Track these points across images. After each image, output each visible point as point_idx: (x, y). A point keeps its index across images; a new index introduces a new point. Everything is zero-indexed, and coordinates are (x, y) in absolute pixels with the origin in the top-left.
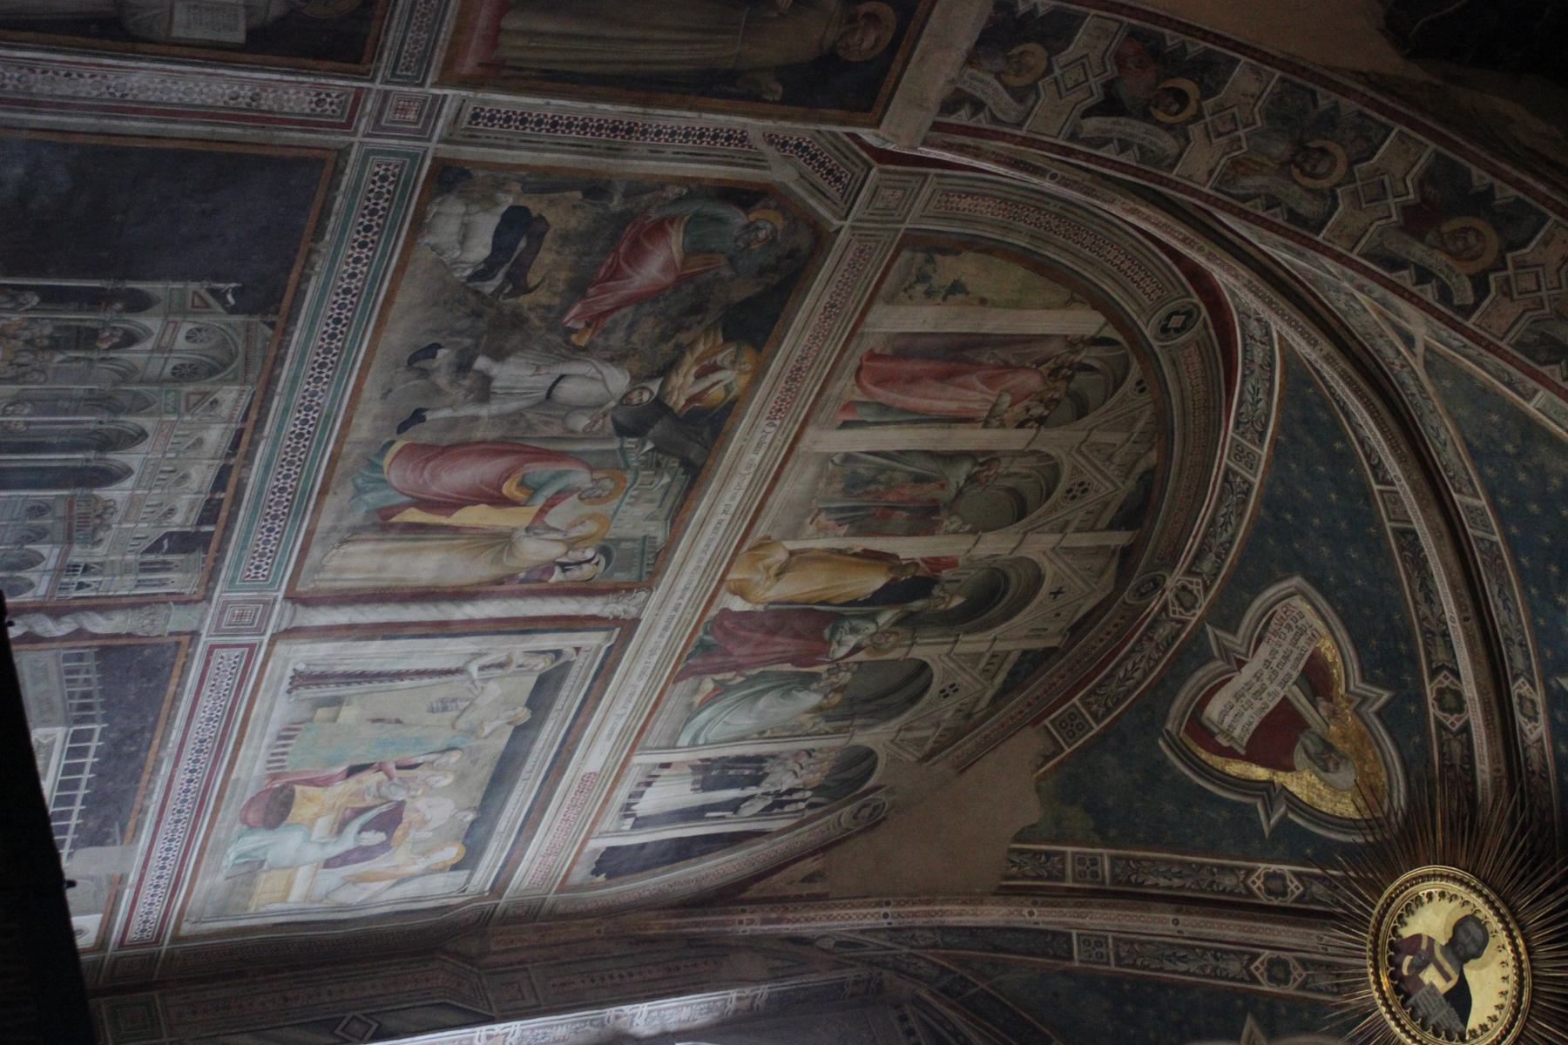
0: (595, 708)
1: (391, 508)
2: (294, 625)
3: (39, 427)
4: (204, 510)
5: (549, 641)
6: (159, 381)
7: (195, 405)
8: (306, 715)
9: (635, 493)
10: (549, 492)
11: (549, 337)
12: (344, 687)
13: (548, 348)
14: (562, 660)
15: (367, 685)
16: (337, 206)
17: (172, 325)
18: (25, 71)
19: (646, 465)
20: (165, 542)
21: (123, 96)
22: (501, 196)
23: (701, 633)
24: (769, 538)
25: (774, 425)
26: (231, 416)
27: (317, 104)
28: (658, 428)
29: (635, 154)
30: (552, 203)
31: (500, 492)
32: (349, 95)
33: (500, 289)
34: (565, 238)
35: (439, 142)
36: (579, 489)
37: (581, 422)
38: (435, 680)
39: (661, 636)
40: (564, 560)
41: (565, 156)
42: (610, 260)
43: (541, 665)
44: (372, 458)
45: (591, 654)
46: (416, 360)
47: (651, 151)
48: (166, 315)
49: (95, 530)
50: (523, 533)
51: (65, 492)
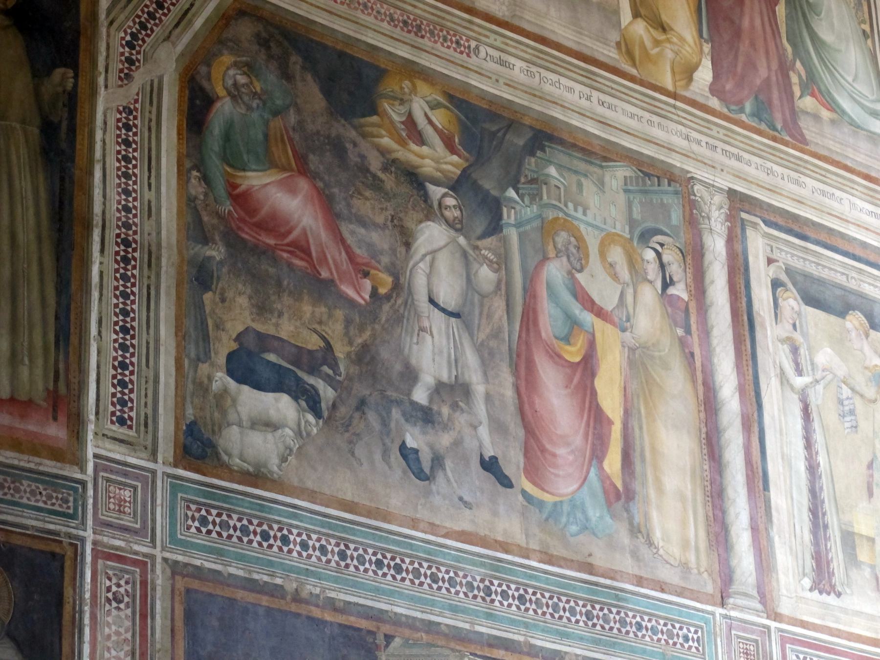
0: (843, 236)
1: (606, 492)
2: (756, 595)
5: (761, 294)
8: (867, 572)
9: (570, 205)
10: (577, 310)
11: (384, 319)
12: (830, 531)
13: (398, 319)
14: (784, 277)
15: (826, 505)
16: (241, 573)
19: (535, 197)
22: (215, 386)
23: (743, 117)
24: (618, 44)
25: (477, 47)
27: (120, 602)
28: (488, 184)
29: (154, 234)
30: (218, 327)
31: (579, 363)
32: (106, 567)
33: (330, 381)
34: (262, 309)
35: (155, 461)
36: (570, 273)
37: (486, 275)
38: (816, 425)
39: (749, 163)
40: (659, 284)
41: (162, 314)
42: (285, 255)
43: (792, 302)
44: (544, 516)
45: (774, 245)
46: (422, 471)
47: (150, 215)
50: (628, 334)
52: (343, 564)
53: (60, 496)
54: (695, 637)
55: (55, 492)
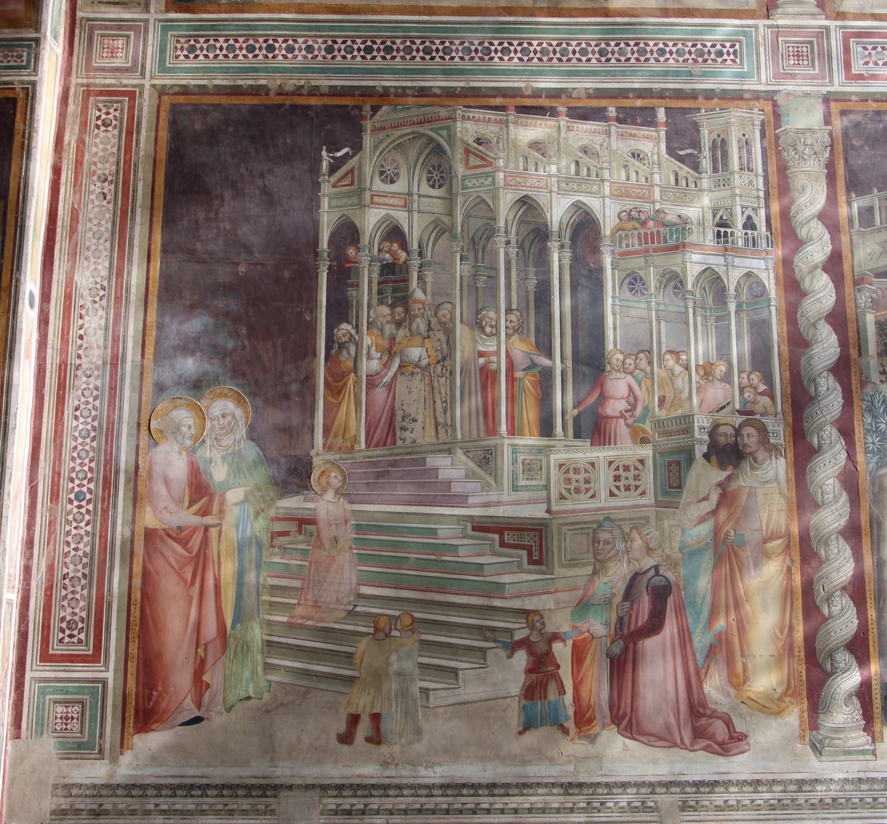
3: (514, 299)
4: (634, 123)
6: (450, 199)
7: (483, 159)
17: (376, 199)
18: (79, 373)
20: (681, 153)
21: (103, 288)
26: (501, 122)
35: (148, 12)
48: (362, 206)
49: (664, 225)
51: (607, 261)
52: (329, 56)
53: (15, 54)
54: (731, 50)
55: (11, 51)
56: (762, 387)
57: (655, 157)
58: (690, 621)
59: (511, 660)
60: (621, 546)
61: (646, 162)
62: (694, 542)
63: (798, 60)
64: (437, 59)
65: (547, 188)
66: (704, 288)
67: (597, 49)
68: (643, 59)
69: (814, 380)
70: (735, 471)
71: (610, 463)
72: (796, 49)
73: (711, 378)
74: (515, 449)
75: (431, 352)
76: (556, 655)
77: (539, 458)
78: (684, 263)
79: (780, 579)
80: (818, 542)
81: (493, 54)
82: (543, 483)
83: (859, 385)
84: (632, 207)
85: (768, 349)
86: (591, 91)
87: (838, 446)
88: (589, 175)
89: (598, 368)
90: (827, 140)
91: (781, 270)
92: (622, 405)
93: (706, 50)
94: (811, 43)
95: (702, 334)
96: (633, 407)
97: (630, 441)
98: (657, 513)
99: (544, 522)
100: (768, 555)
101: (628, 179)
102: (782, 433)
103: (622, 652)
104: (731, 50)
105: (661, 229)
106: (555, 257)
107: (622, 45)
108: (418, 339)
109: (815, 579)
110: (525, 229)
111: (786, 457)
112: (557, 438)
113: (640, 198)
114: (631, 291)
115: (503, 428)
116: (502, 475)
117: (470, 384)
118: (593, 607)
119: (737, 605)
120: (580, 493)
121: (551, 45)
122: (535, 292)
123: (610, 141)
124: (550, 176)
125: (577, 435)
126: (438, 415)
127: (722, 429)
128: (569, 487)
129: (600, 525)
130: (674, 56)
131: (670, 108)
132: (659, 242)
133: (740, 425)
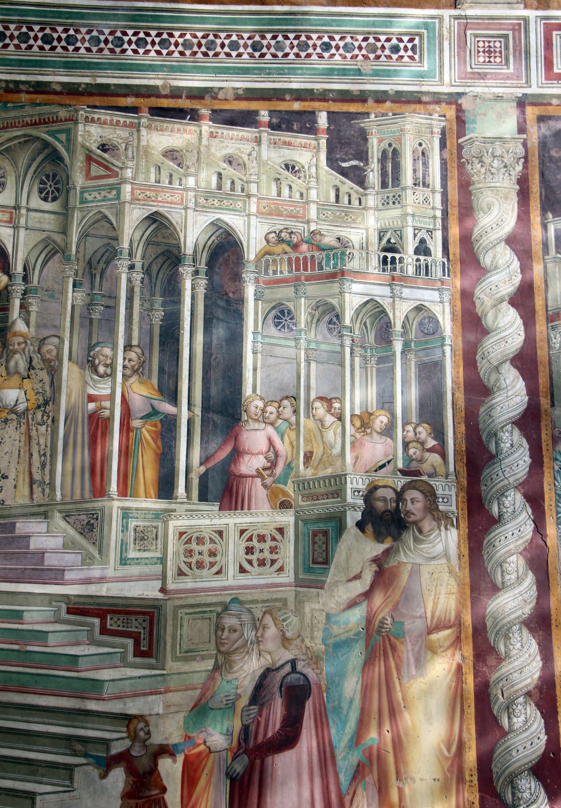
4: (290, 129)
7: (107, 168)
20: (345, 165)
26: (131, 125)
49: (321, 249)
51: (250, 291)
54: (410, 45)
56: (431, 443)
57: (313, 170)
58: (333, 731)
59: (104, 781)
60: (249, 634)
61: (302, 175)
62: (342, 631)
63: (490, 57)
64: (59, 50)
65: (182, 203)
66: (365, 324)
67: (250, 42)
68: (303, 54)
69: (496, 435)
70: (395, 544)
71: (242, 532)
72: (487, 44)
73: (368, 431)
74: (126, 513)
75: (31, 395)
76: (163, 774)
77: (154, 524)
78: (341, 293)
79: (448, 679)
80: (497, 633)
81: (126, 46)
82: (159, 555)
83: (550, 442)
84: (282, 227)
85: (440, 395)
86: (240, 92)
87: (524, 515)
88: (232, 189)
89: (233, 416)
90: (520, 151)
91: (459, 304)
92: (259, 462)
93: (379, 45)
94: (506, 37)
95: (361, 377)
96: (273, 465)
97: (267, 505)
98: (297, 594)
99: (156, 603)
100: (433, 649)
101: (279, 194)
102: (454, 498)
103: (245, 772)
104: (410, 45)
105: (317, 254)
106: (188, 284)
107: (280, 38)
108: (16, 379)
109: (492, 680)
110: (153, 251)
111: (458, 528)
112: (179, 500)
113: (293, 217)
114: (277, 326)
115: (114, 487)
116: (109, 545)
117: (75, 434)
118: (212, 713)
119: (393, 713)
120: (204, 567)
121: (196, 37)
122: (161, 326)
123: (260, 150)
124: (186, 190)
125: (203, 497)
126: (34, 470)
127: (380, 493)
128: (190, 560)
129: (226, 607)
130: (341, 51)
131: (333, 112)
132: (313, 269)
133: (402, 488)
